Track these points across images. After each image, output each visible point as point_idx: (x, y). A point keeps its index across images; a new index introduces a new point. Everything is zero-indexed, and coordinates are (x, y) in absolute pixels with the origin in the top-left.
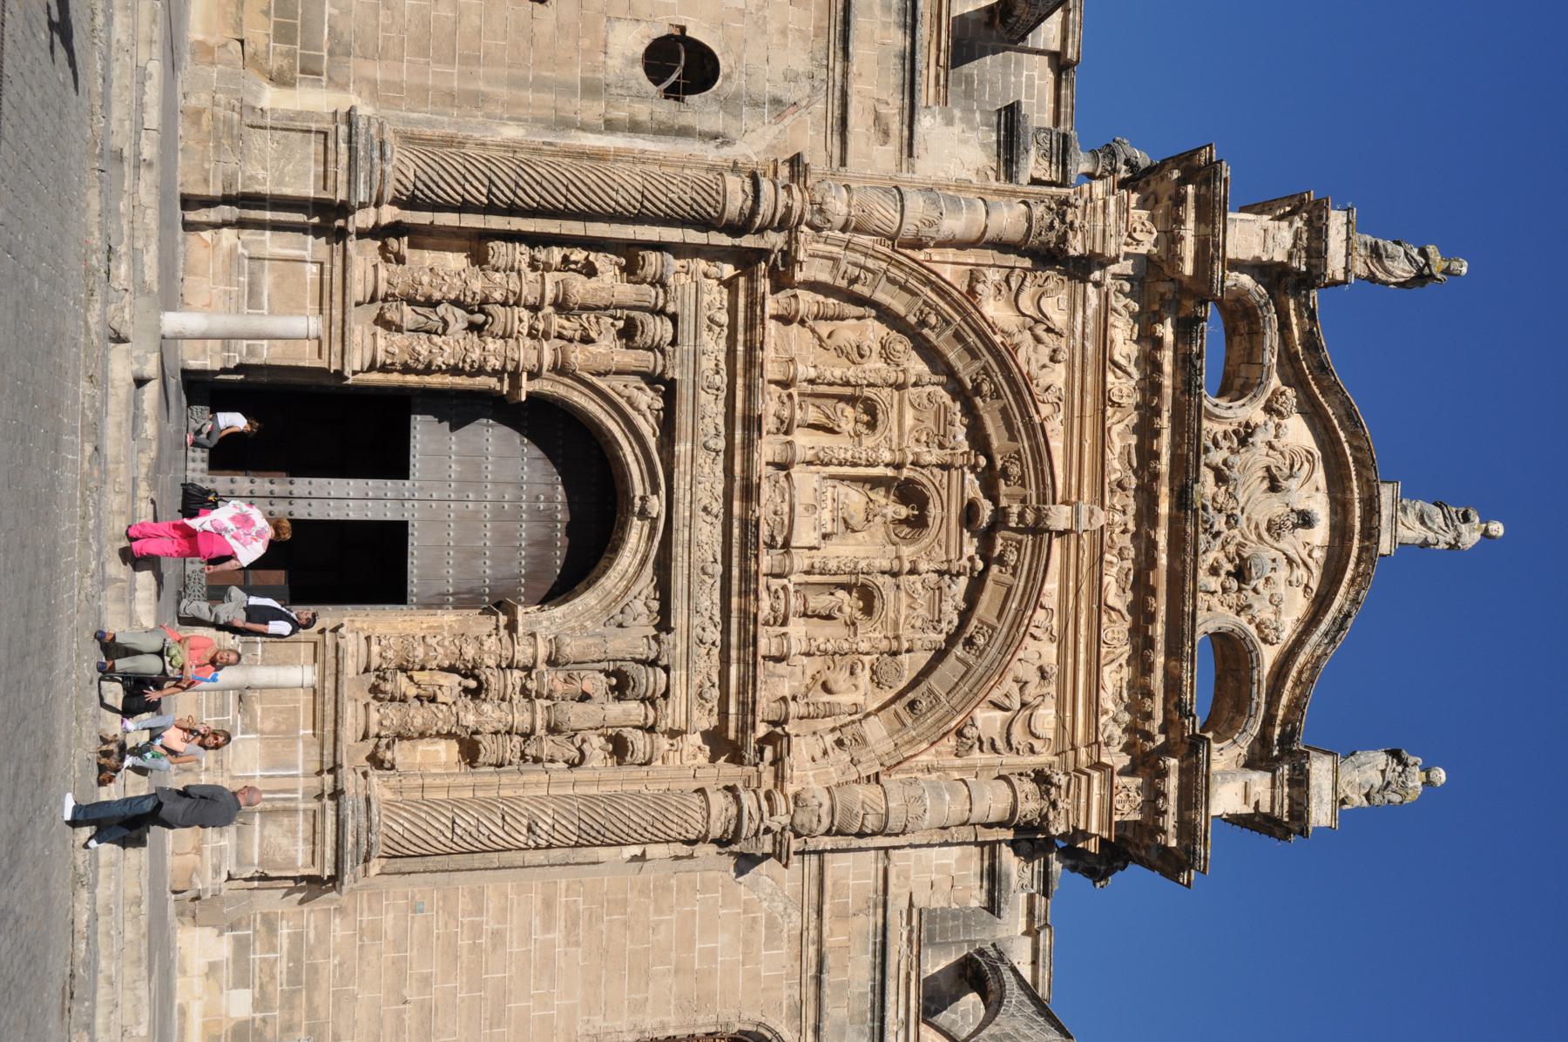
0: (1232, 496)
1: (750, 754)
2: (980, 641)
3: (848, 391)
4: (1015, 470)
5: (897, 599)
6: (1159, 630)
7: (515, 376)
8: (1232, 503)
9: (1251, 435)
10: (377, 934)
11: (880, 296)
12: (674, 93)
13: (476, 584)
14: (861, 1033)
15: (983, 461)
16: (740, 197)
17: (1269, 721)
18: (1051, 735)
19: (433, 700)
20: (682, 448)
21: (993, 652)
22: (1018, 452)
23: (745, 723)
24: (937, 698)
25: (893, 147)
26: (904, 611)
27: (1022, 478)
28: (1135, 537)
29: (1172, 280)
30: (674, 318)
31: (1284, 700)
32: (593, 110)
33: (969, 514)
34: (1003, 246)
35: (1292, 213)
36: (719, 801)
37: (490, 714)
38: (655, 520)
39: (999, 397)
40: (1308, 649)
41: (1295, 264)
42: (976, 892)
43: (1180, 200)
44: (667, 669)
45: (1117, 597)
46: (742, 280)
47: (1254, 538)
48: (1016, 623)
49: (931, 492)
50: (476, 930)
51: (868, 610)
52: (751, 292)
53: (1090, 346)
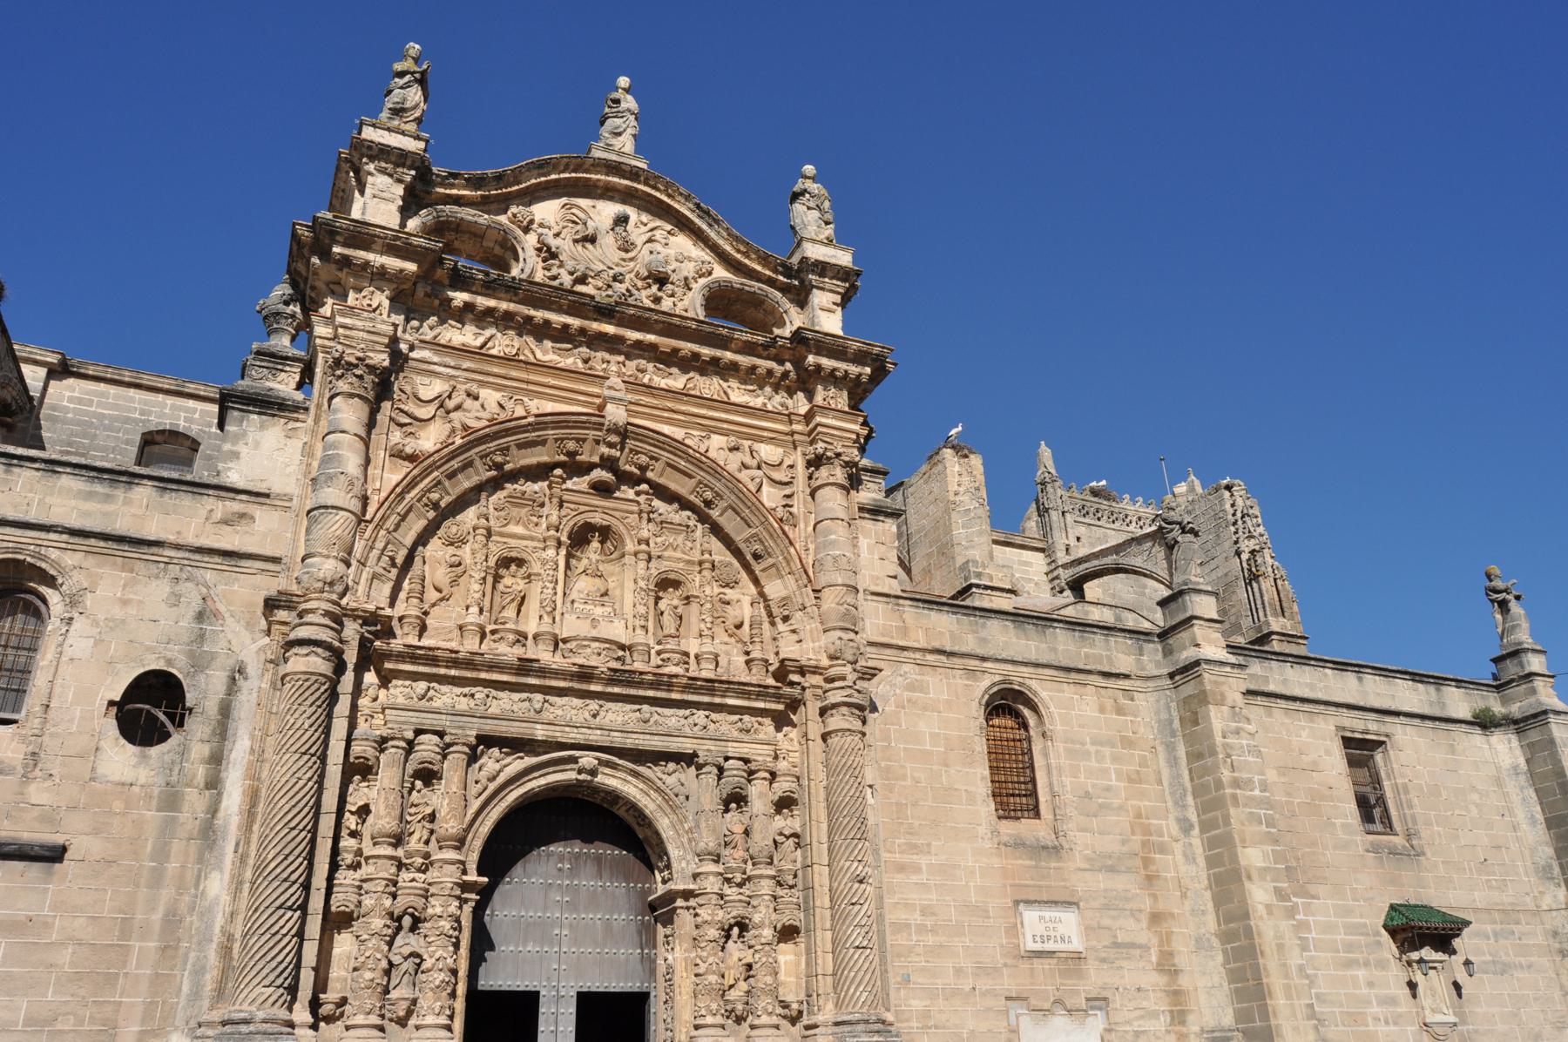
0: (598, 274)
1: (796, 691)
2: (709, 495)
3: (490, 579)
4: (571, 445)
5: (669, 559)
6: (706, 351)
7: (466, 887)
8: (604, 275)
9: (549, 249)
10: (926, 1014)
11: (409, 540)
13: (633, 928)
14: (984, 626)
15: (558, 472)
16: (313, 658)
17: (771, 282)
18: (781, 450)
19: (749, 967)
20: (540, 733)
21: (718, 486)
22: (556, 440)
23: (774, 695)
24: (753, 536)
25: (258, 512)
26: (679, 555)
27: (577, 440)
28: (628, 357)
29: (415, 284)
30: (418, 732)
31: (759, 268)
32: (194, 801)
33: (602, 489)
34: (371, 424)
35: (357, 171)
36: (836, 721)
37: (764, 918)
38: (601, 762)
39: (507, 449)
40: (721, 242)
41: (408, 179)
42: (887, 526)
43: (346, 262)
44: (727, 759)
45: (678, 381)
46: (388, 665)
47: (632, 264)
48: (698, 464)
49: (581, 519)
50: (921, 929)
51: (676, 584)
52: (401, 657)
53: (466, 365)
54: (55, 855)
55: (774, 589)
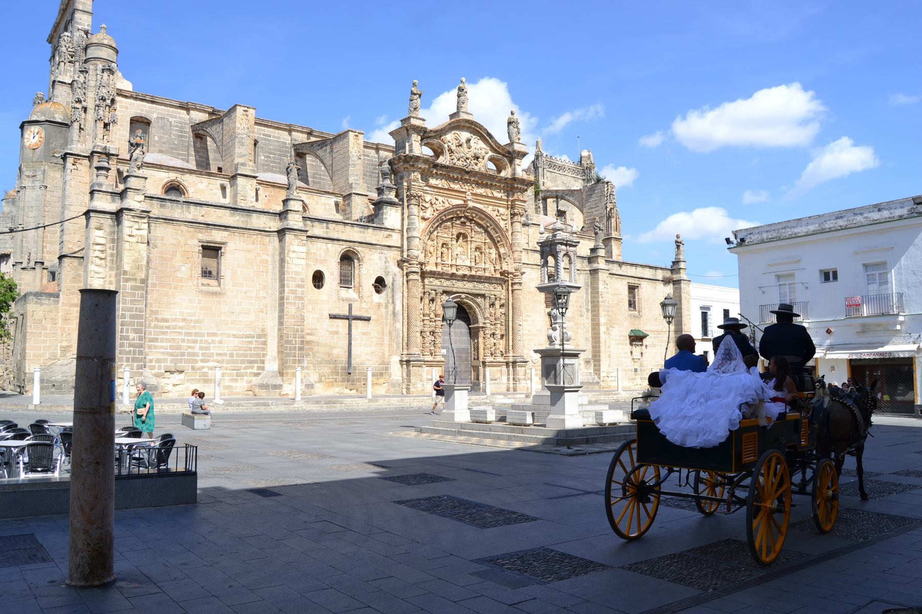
12: (385, 286)
17: (504, 155)
20: (455, 290)
33: (463, 224)
36: (516, 287)
54: (368, 319)
55: (502, 250)
